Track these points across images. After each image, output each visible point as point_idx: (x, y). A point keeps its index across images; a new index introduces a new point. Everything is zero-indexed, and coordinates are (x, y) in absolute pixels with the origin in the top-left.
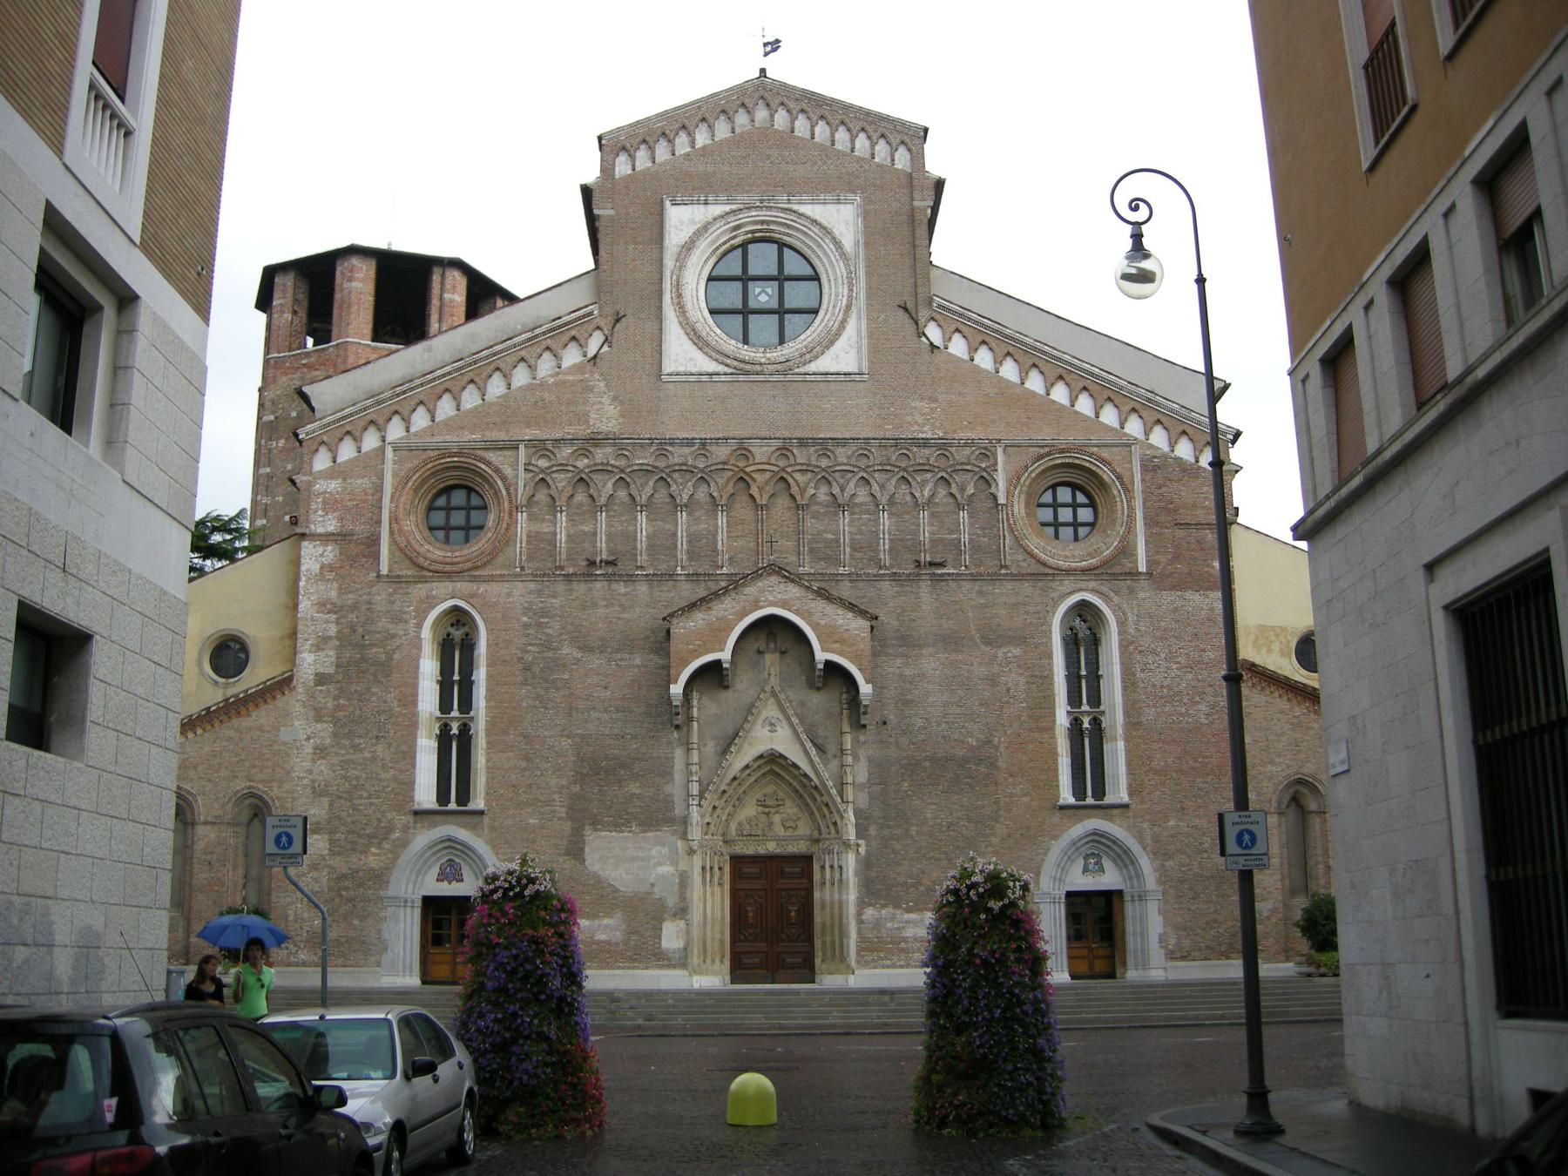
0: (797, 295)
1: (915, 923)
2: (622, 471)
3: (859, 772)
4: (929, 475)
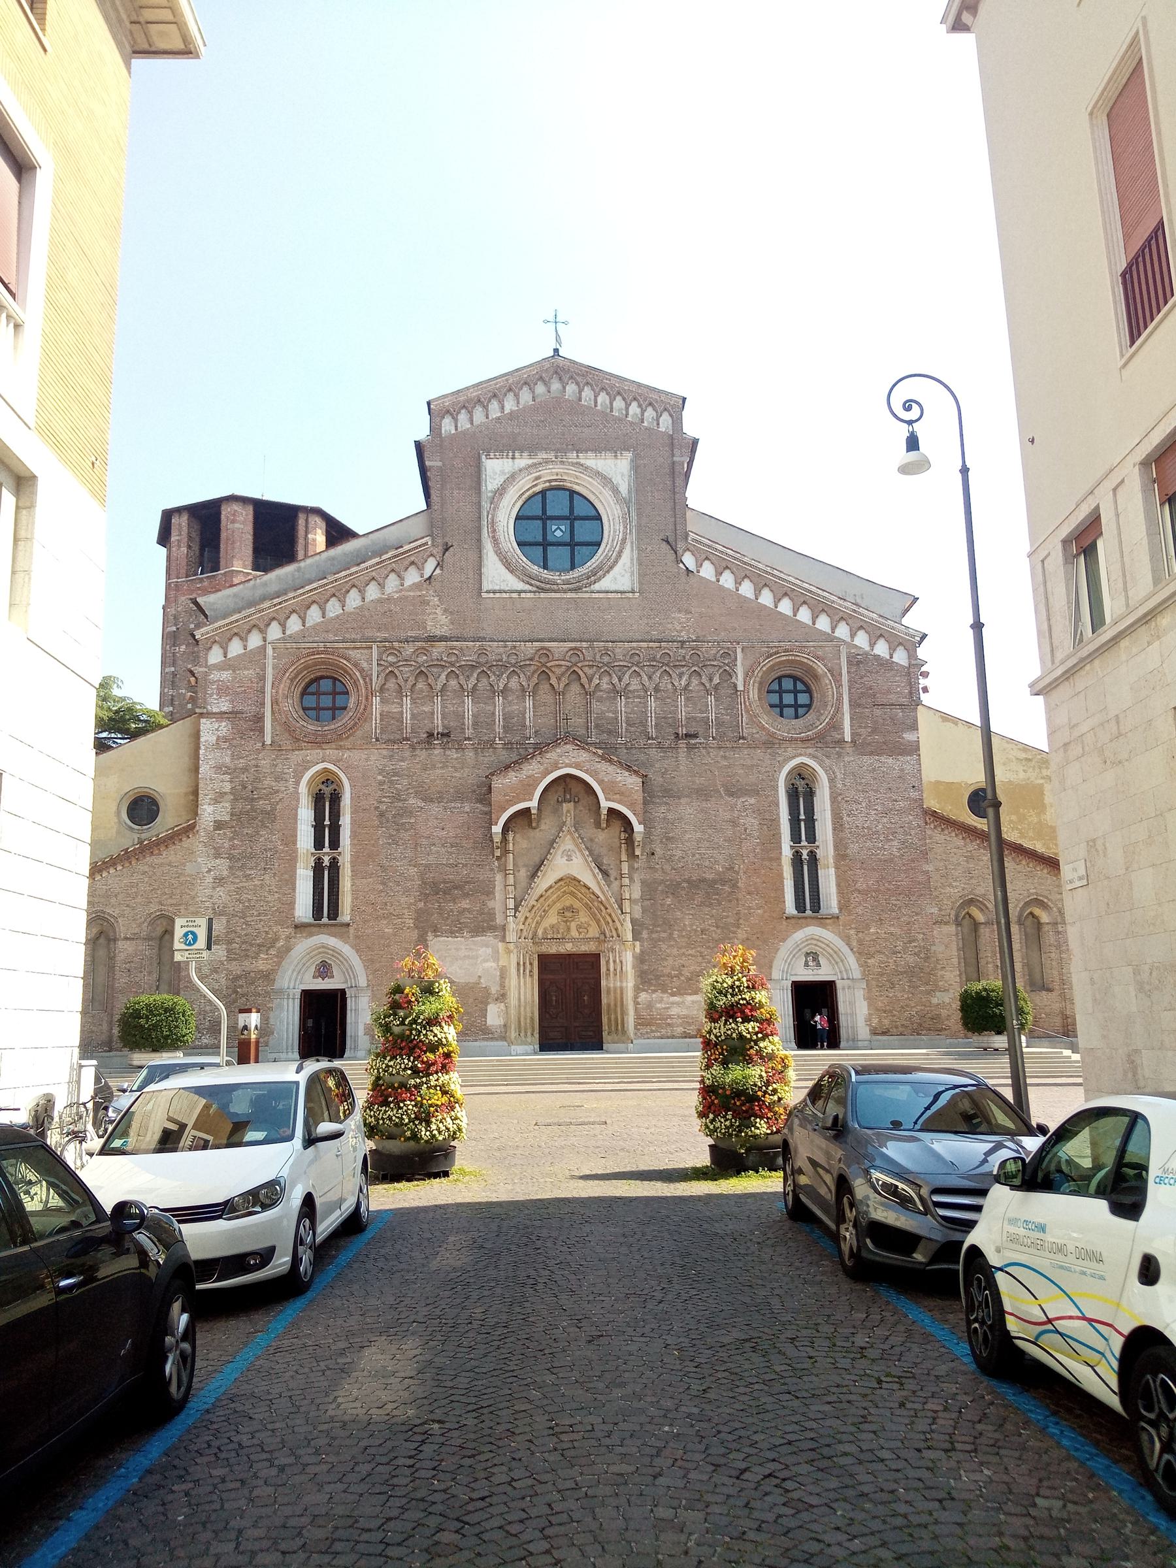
0: (584, 531)
1: (678, 1004)
2: (453, 665)
4: (684, 669)
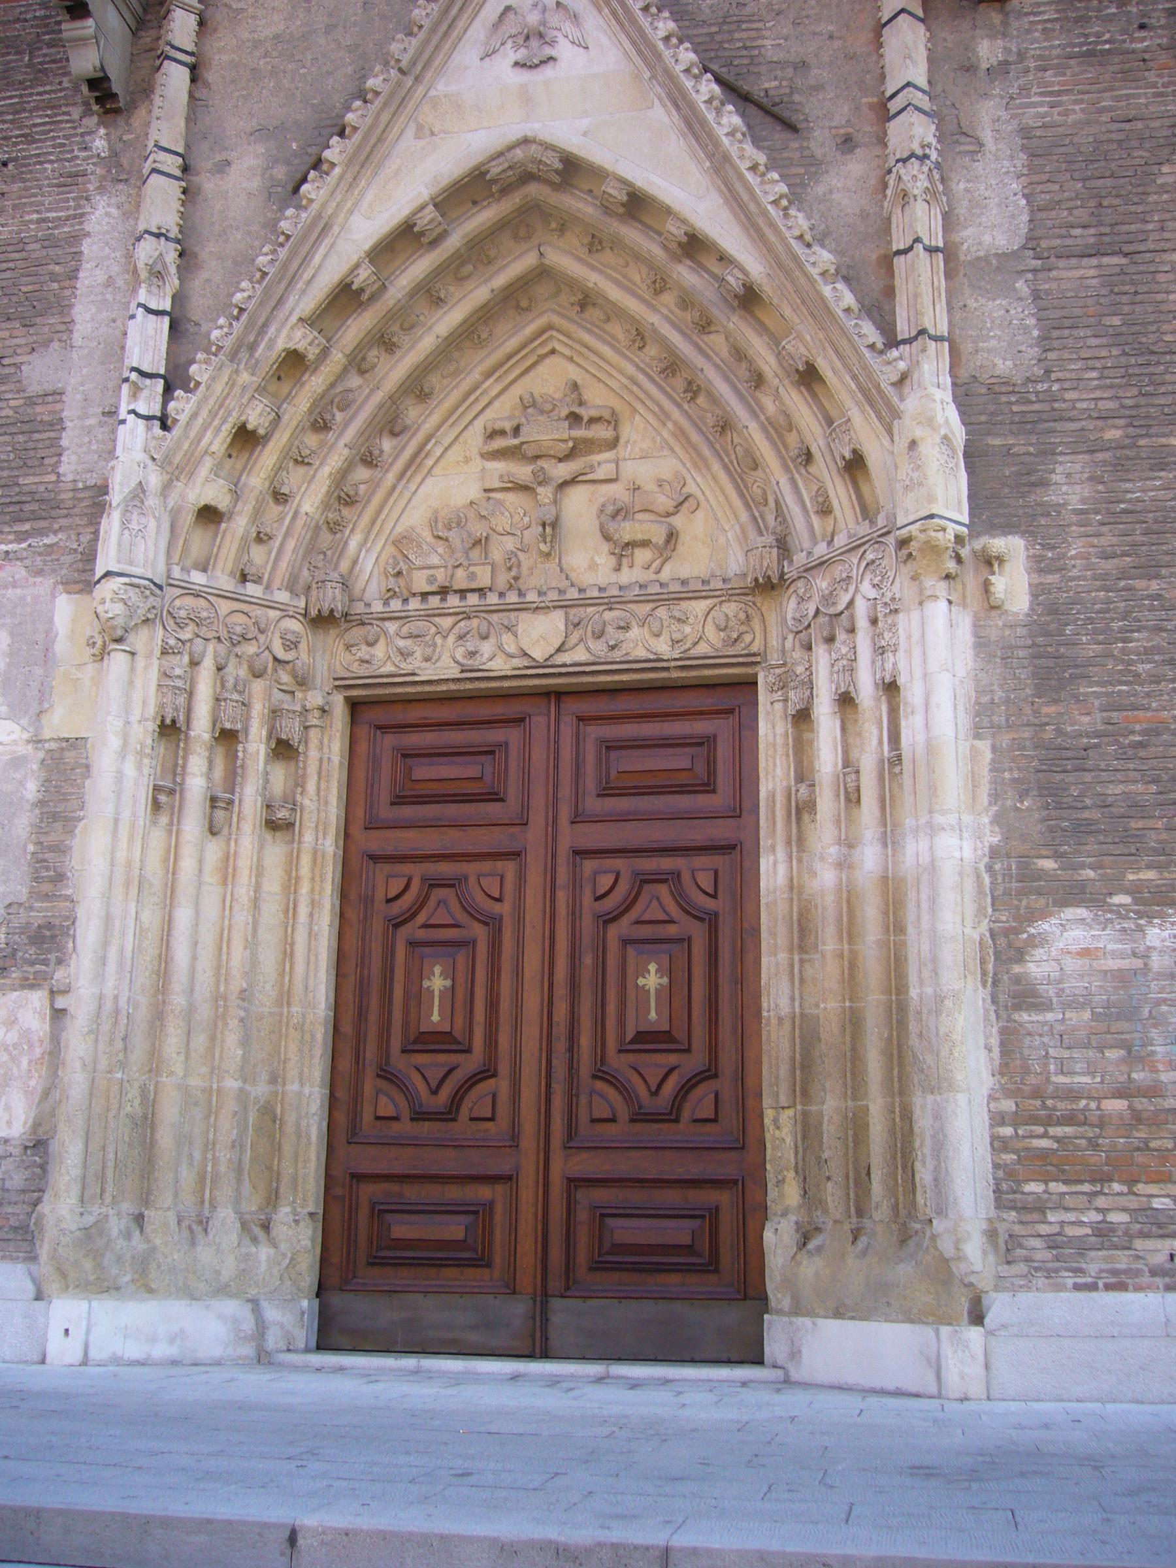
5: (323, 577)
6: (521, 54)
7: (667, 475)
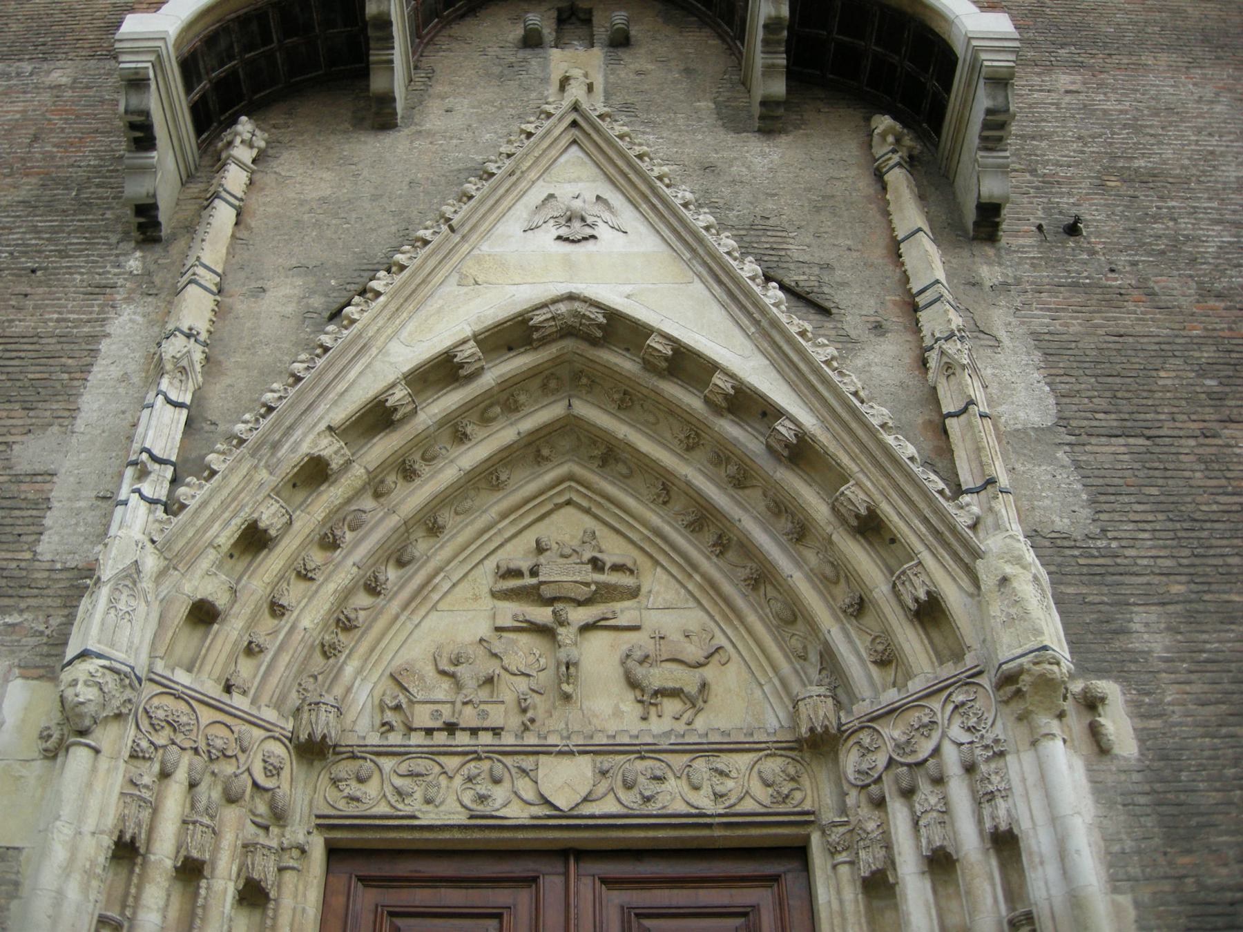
3: (1009, 388)
5: (318, 699)
6: (564, 231)
7: (693, 626)
